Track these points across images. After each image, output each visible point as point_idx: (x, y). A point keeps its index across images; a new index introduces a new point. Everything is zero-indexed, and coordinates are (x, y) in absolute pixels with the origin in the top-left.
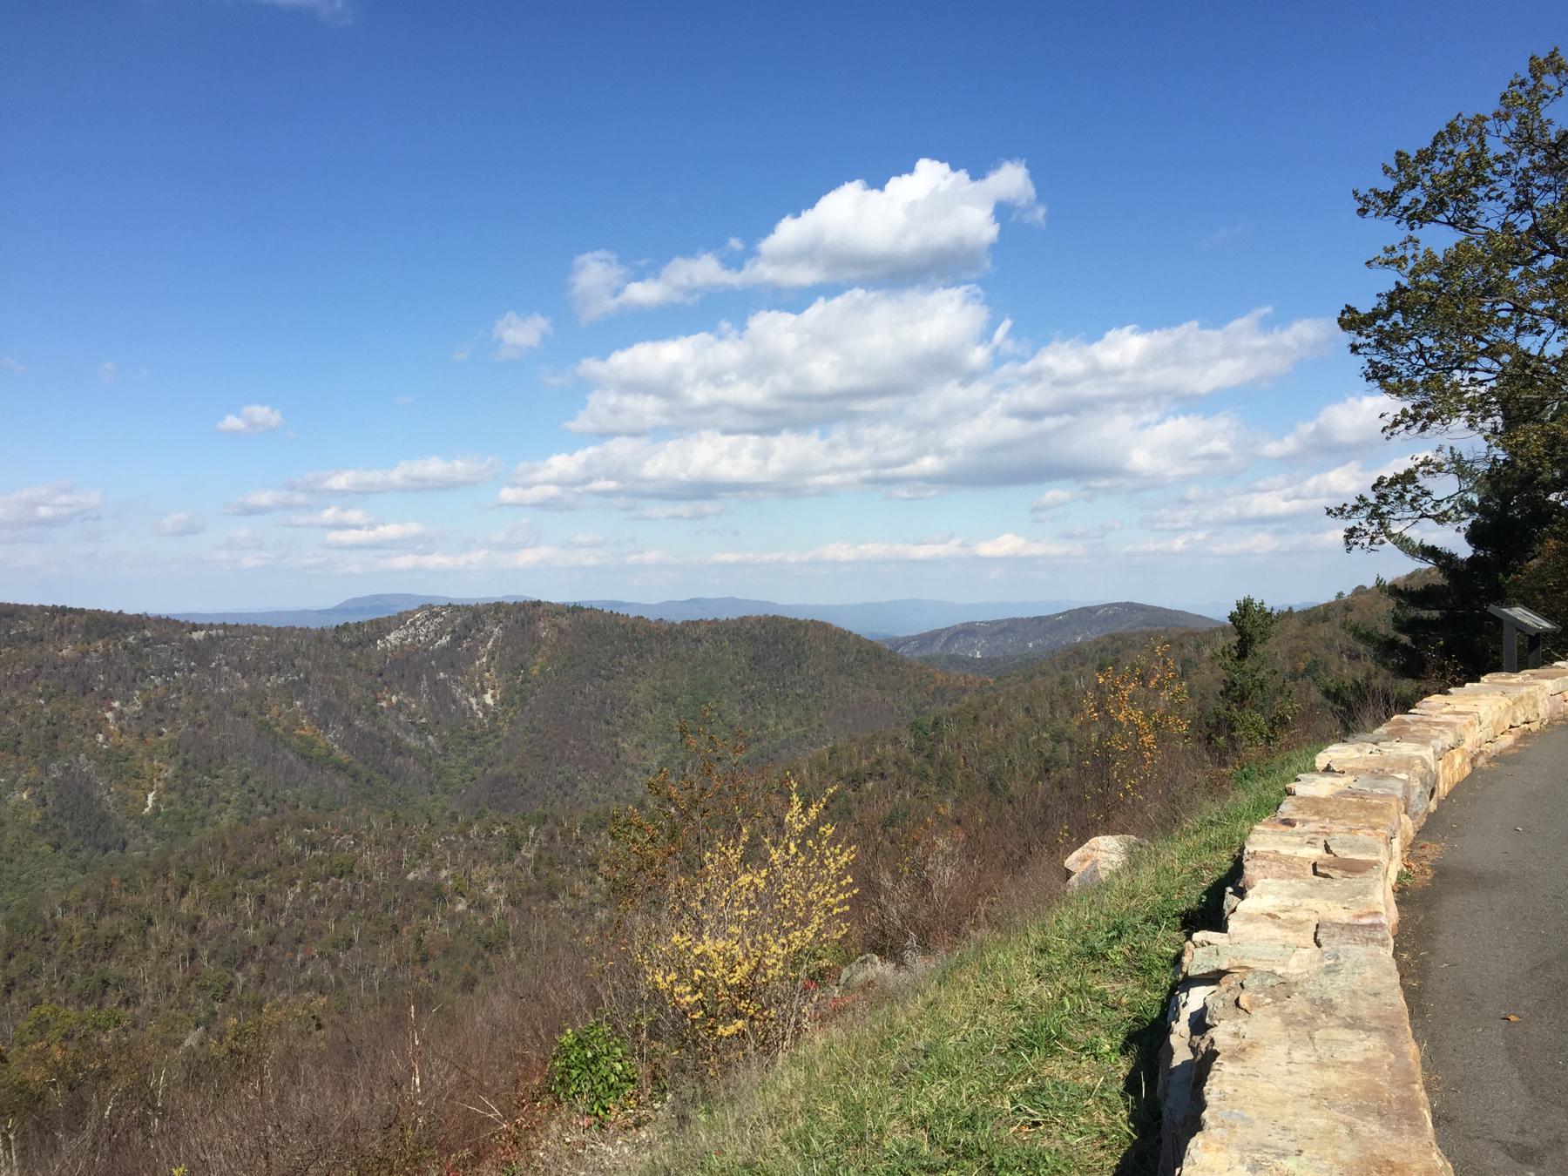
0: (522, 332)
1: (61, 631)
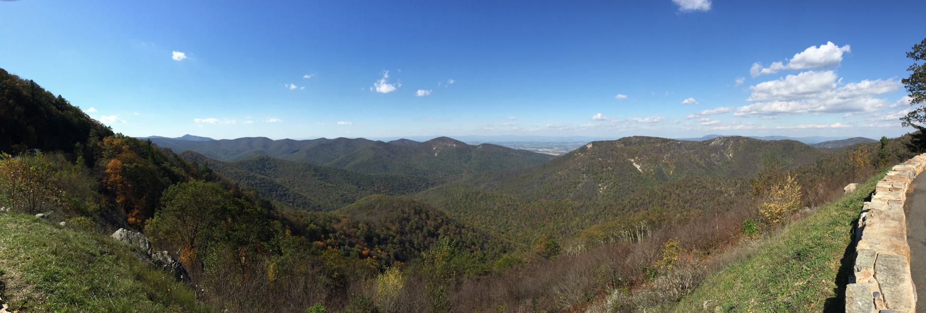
0: (739, 81)
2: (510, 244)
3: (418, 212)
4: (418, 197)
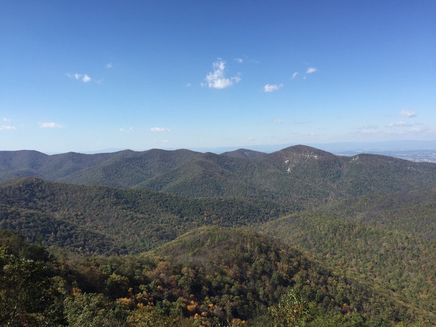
2: (406, 309)
3: (264, 250)
4: (264, 229)
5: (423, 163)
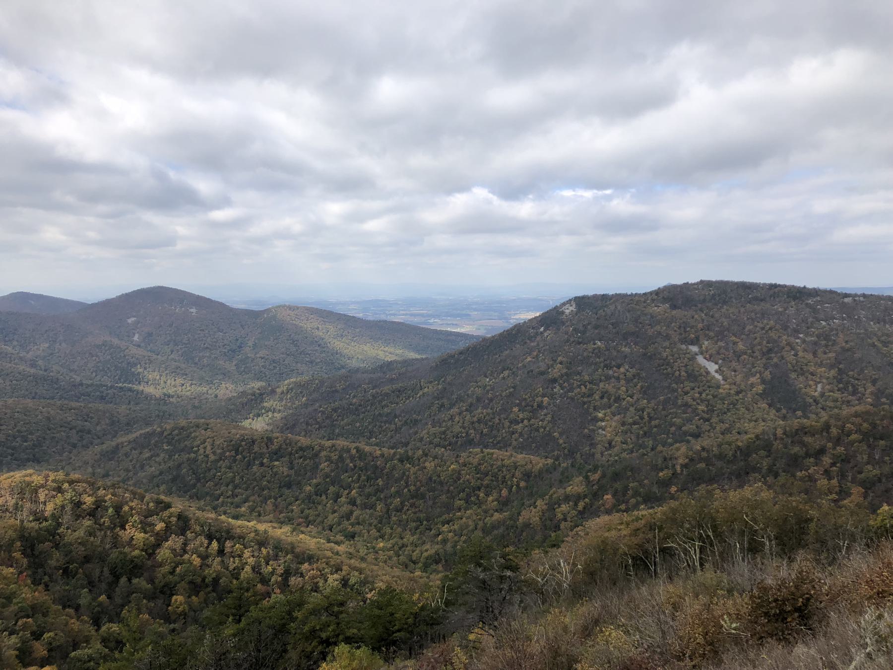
1: (774, 296)
5: (380, 321)
